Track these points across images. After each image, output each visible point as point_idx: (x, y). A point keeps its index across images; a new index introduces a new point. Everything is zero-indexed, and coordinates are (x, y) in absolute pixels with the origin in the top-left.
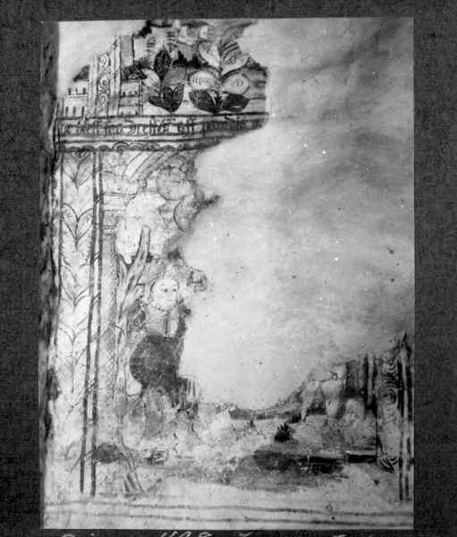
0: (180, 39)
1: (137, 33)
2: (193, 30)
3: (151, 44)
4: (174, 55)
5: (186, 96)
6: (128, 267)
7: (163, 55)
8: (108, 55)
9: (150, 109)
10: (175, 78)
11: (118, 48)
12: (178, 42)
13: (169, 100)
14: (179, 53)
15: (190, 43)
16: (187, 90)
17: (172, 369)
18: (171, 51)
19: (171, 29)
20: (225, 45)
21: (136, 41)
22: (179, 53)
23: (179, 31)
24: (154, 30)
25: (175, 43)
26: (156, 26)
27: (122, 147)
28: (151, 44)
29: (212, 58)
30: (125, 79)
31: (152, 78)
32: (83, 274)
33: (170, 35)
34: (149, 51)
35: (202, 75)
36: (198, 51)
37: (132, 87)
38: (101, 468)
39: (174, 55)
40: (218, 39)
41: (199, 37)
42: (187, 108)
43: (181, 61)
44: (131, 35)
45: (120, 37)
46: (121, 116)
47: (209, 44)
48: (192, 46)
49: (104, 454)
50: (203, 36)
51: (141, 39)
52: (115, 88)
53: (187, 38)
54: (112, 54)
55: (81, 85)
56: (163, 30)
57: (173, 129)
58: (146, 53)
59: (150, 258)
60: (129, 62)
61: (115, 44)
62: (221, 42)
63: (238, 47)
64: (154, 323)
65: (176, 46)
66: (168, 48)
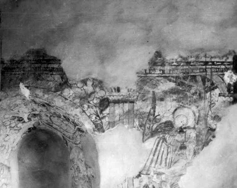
0: (153, 180)
1: (135, 177)
2: (159, 176)
3: (141, 182)
8: (122, 184)
11: (126, 183)
12: (153, 181)
14: (153, 186)
15: (158, 182)
18: (149, 184)
19: (150, 176)
20: (173, 184)
21: (134, 180)
22: (153, 186)
23: (153, 177)
24: (142, 176)
25: (151, 181)
26: (143, 174)
28: (141, 182)
33: (149, 178)
34: (140, 184)
36: (161, 186)
40: (170, 181)
41: (161, 180)
44: (132, 177)
45: (127, 178)
47: (166, 183)
48: (159, 184)
50: (164, 179)
51: (137, 179)
53: (156, 179)
54: (124, 184)
56: (146, 176)
58: (139, 185)
61: (125, 180)
62: (171, 183)
63: (178, 186)
65: (151, 183)
66: (148, 184)
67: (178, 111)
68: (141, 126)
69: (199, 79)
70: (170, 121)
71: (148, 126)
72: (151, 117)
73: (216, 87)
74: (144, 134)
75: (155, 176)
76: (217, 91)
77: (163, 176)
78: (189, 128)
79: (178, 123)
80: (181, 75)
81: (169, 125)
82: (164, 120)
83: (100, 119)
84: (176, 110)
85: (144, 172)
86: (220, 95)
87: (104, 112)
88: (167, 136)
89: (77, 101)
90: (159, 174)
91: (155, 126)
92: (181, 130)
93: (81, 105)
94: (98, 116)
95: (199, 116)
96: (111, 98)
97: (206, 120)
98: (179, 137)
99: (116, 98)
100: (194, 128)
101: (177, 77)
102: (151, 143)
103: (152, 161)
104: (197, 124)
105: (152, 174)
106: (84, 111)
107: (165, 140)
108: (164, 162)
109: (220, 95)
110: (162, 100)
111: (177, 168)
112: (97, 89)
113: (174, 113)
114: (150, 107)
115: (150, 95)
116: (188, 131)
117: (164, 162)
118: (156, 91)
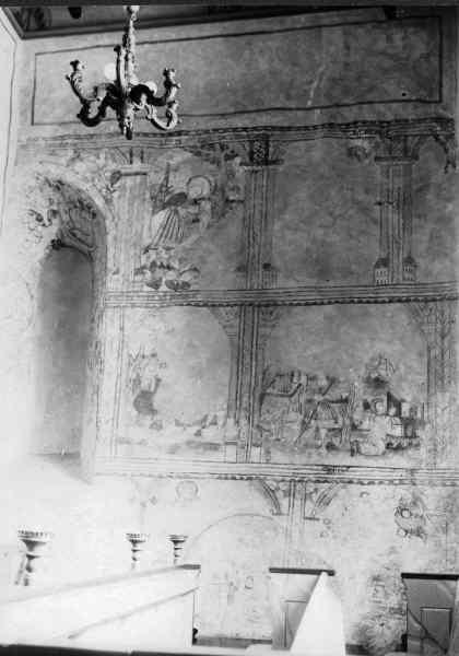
3: (148, 258)
4: (159, 263)
5: (163, 283)
6: (134, 360)
7: (153, 264)
9: (146, 289)
10: (159, 273)
13: (155, 285)
16: (164, 280)
17: (151, 405)
27: (133, 306)
28: (148, 258)
29: (176, 265)
30: (136, 274)
31: (148, 274)
32: (114, 363)
33: (157, 254)
35: (171, 272)
37: (139, 278)
38: (119, 447)
39: (159, 263)
42: (164, 288)
43: (162, 266)
46: (134, 292)
49: (121, 441)
52: (131, 279)
55: (116, 276)
57: (157, 298)
59: (144, 357)
60: (138, 266)
64: (144, 385)
67: (193, 181)
68: (152, 198)
69: (218, 146)
70: (183, 194)
71: (159, 198)
72: (164, 189)
73: (237, 155)
74: (155, 207)
75: (164, 251)
76: (238, 160)
77: (172, 251)
78: (203, 199)
79: (193, 194)
80: (199, 145)
81: (183, 197)
82: (177, 192)
83: (112, 192)
84: (190, 180)
85: (153, 247)
86: (241, 164)
87: (116, 186)
88: (179, 208)
89: (88, 175)
90: (168, 249)
91: (167, 198)
92: (195, 202)
93: (93, 180)
94: (108, 189)
95: (216, 185)
96: (123, 171)
97: (223, 192)
98: (193, 210)
99: (128, 171)
100: (209, 199)
101: (195, 147)
102: (161, 216)
103: (162, 235)
104: (213, 193)
105: (160, 249)
106: (94, 185)
107: (176, 212)
108: (174, 237)
109: (241, 164)
110: (176, 170)
111: (187, 243)
112: (110, 162)
113: (188, 183)
114: (163, 178)
115: (164, 166)
116: (203, 203)
117: (174, 237)
118: (171, 162)
